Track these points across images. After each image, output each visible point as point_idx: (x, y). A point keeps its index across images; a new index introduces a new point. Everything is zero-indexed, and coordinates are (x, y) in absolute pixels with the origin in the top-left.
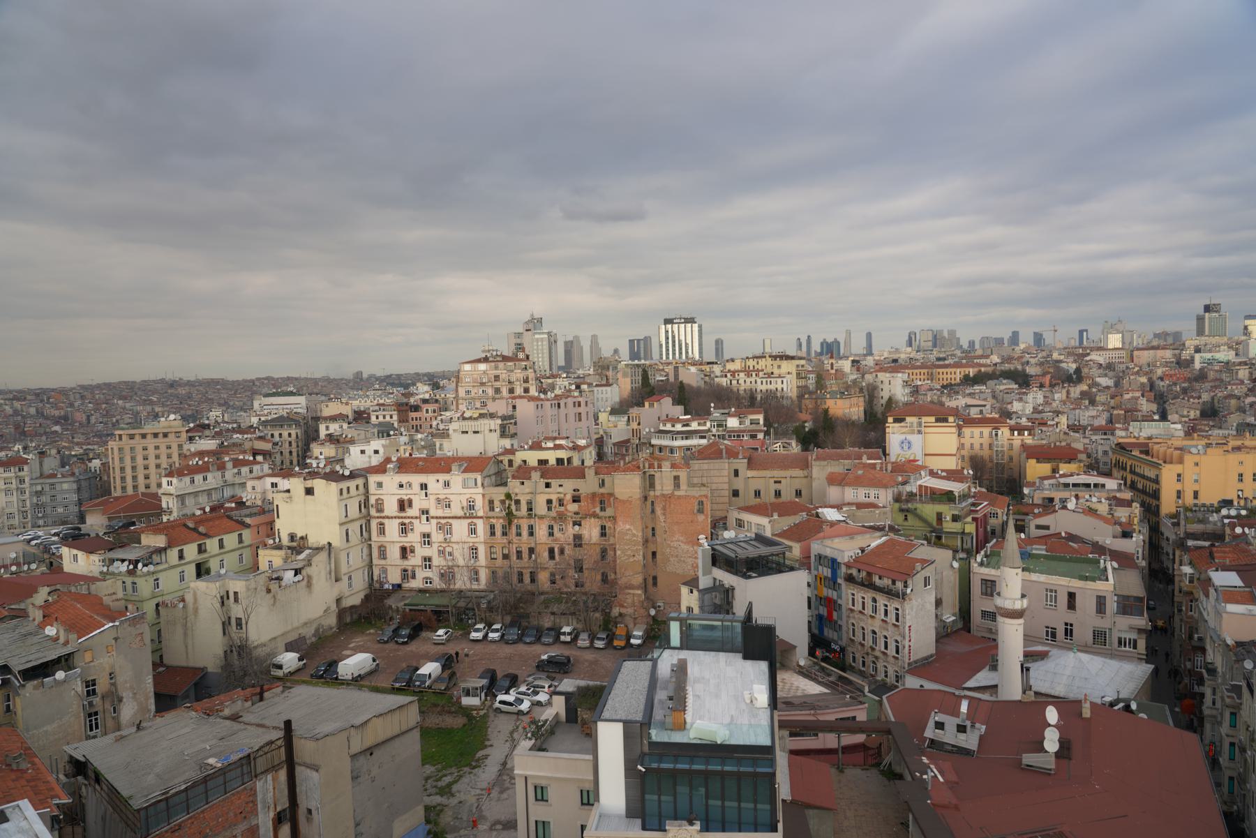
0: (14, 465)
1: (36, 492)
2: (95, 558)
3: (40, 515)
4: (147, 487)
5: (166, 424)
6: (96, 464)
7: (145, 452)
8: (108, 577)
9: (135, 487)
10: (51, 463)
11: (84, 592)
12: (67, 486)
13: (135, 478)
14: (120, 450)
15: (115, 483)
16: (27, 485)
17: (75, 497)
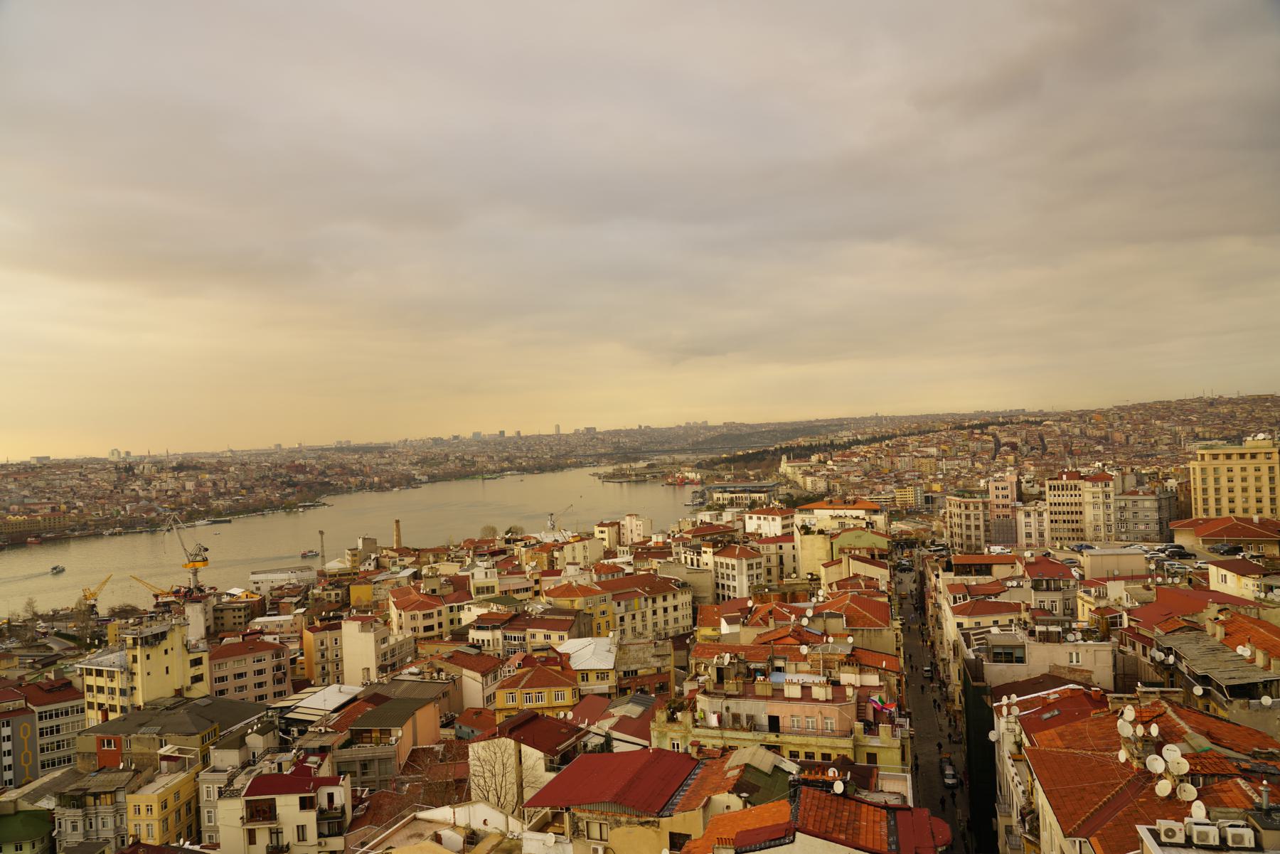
0: (1102, 481)
1: (1120, 508)
2: (1245, 580)
3: (1123, 530)
4: (1232, 511)
5: (1254, 444)
6: (1172, 483)
7: (1230, 474)
8: (1264, 603)
9: (1218, 511)
10: (1131, 481)
11: (1253, 615)
12: (1149, 503)
13: (1218, 501)
14: (1203, 470)
15: (1196, 504)
16: (1111, 500)
17: (1156, 516)
